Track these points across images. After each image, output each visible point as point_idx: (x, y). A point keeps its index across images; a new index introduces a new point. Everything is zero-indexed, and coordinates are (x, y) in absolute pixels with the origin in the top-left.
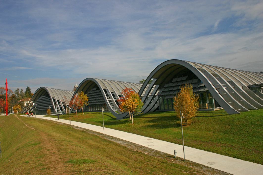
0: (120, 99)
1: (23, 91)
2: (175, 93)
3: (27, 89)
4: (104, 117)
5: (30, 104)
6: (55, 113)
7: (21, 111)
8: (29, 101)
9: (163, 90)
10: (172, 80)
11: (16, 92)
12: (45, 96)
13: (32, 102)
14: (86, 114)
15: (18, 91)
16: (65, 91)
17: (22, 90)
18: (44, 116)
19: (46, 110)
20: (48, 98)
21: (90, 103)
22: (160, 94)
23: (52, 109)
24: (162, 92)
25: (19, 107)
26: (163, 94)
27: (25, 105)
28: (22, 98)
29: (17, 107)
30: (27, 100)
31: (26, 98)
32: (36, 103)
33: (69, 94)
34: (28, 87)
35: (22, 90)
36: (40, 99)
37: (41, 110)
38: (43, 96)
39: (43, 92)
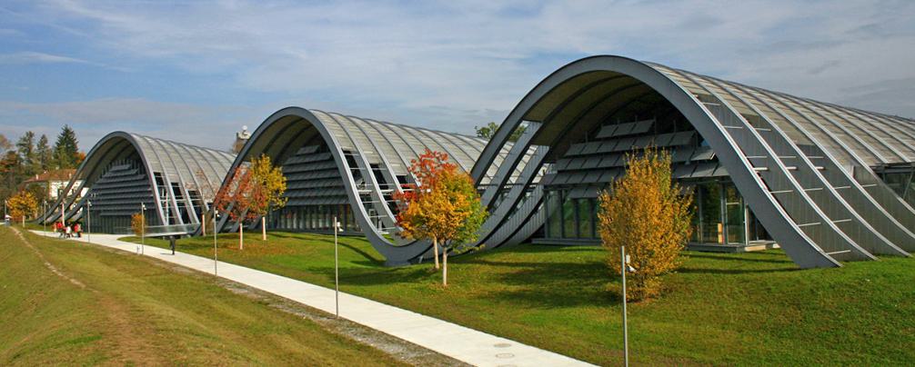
0: (401, 191)
1: (46, 141)
2: (604, 179)
3: (63, 135)
4: (339, 255)
5: (70, 193)
6: (163, 230)
7: (36, 215)
8: (67, 180)
9: (562, 165)
10: (597, 129)
11: (21, 145)
12: (127, 167)
13: (78, 184)
14: (276, 239)
15: (30, 144)
16: (202, 149)
17: (43, 137)
18: (119, 239)
19: (130, 217)
20: (137, 174)
21: (290, 198)
22: (548, 182)
23: (152, 214)
24: (559, 172)
25: (29, 199)
26: (562, 180)
27: (54, 194)
28: (44, 167)
29: (23, 202)
30: (62, 178)
31: (57, 168)
32: (94, 190)
33: (216, 163)
34: (68, 127)
35: (44, 140)
36: (107, 175)
37: (111, 216)
38: (122, 164)
39: (121, 150)
